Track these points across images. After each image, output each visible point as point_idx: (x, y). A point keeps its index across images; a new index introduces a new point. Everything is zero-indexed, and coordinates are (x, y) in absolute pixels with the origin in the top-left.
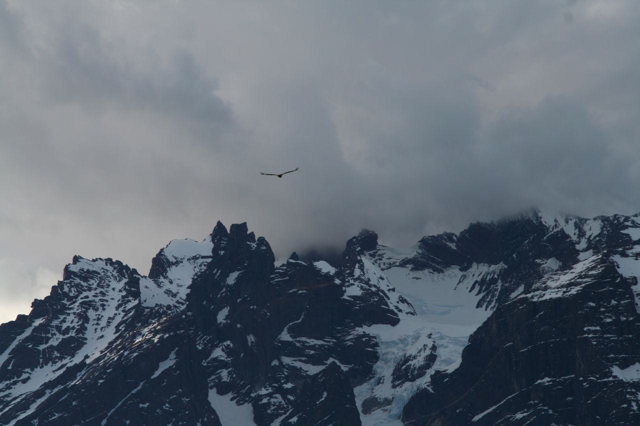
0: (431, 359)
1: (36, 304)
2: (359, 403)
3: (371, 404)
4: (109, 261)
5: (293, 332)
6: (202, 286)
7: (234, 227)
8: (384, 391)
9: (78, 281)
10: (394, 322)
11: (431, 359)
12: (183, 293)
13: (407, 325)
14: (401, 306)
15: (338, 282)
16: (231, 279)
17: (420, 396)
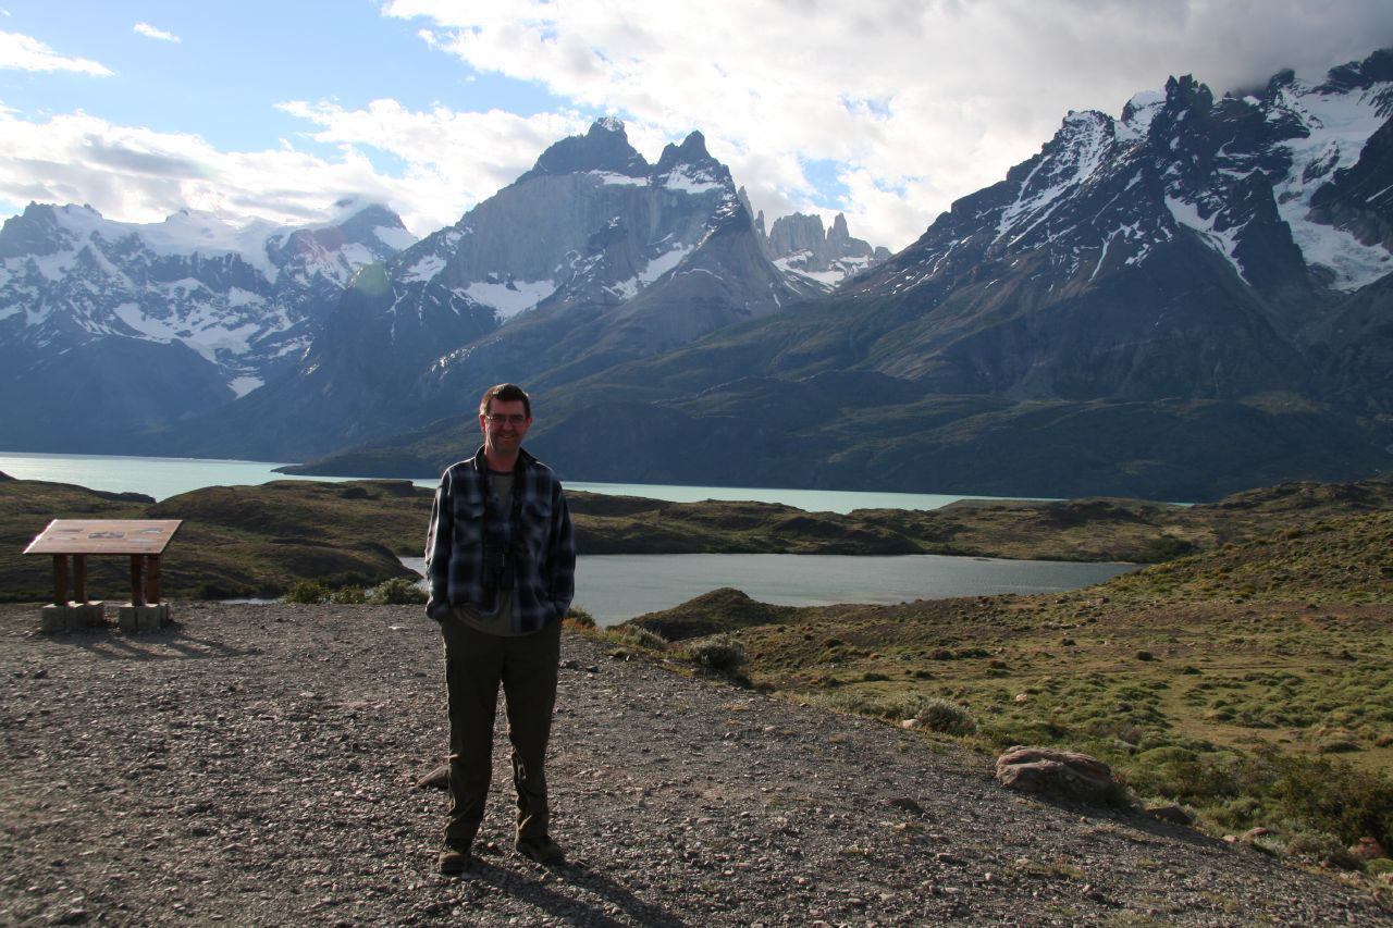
0: (1335, 160)
1: (1045, 146)
2: (1276, 197)
3: (1285, 197)
4: (1093, 112)
5: (1228, 150)
6: (1160, 125)
7: (1182, 78)
8: (1295, 187)
9: (1071, 128)
10: (1305, 134)
11: (1335, 160)
12: (1146, 129)
13: (1316, 136)
14: (1312, 123)
15: (1261, 110)
16: (1180, 117)
17: (1326, 187)
